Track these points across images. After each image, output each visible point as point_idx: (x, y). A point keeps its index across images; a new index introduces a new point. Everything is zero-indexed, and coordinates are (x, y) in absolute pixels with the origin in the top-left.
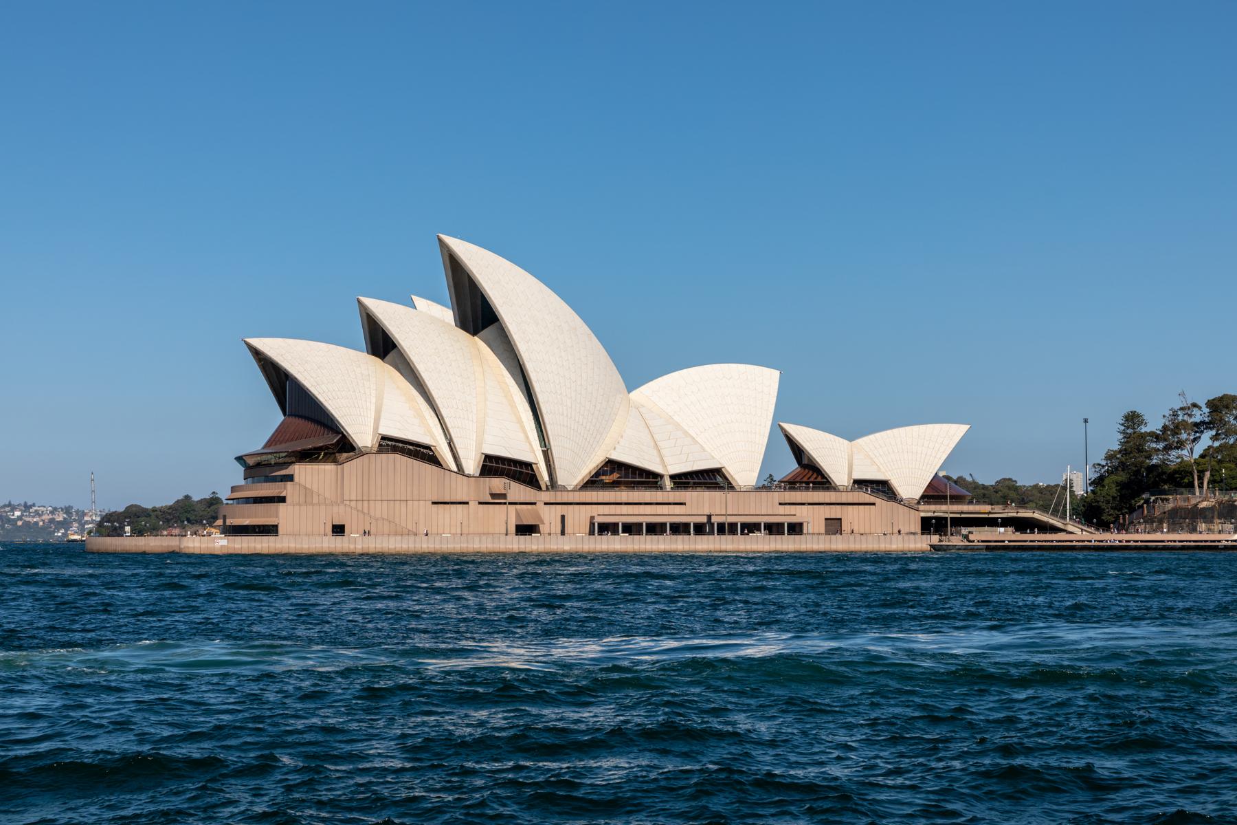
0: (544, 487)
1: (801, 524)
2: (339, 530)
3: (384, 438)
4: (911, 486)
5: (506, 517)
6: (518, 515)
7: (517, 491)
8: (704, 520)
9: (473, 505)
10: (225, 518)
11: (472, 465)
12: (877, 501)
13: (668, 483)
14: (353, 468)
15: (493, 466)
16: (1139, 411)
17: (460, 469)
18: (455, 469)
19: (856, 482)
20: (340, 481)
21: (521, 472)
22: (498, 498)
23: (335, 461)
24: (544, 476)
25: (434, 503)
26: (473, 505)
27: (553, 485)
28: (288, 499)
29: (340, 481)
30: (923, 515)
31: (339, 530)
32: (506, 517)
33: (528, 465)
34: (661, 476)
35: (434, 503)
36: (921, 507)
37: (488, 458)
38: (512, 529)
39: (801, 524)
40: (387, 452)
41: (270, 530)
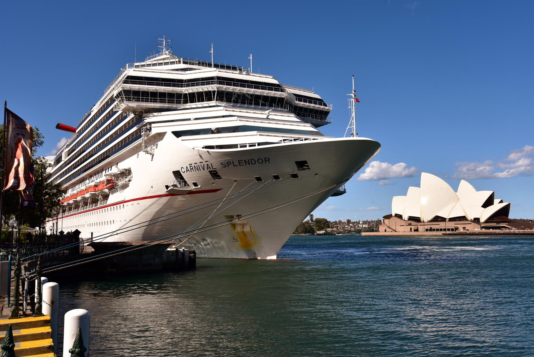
4: (482, 220)
7: (413, 223)
11: (406, 219)
13: (447, 220)
21: (417, 220)
22: (410, 224)
27: (423, 222)
34: (446, 219)
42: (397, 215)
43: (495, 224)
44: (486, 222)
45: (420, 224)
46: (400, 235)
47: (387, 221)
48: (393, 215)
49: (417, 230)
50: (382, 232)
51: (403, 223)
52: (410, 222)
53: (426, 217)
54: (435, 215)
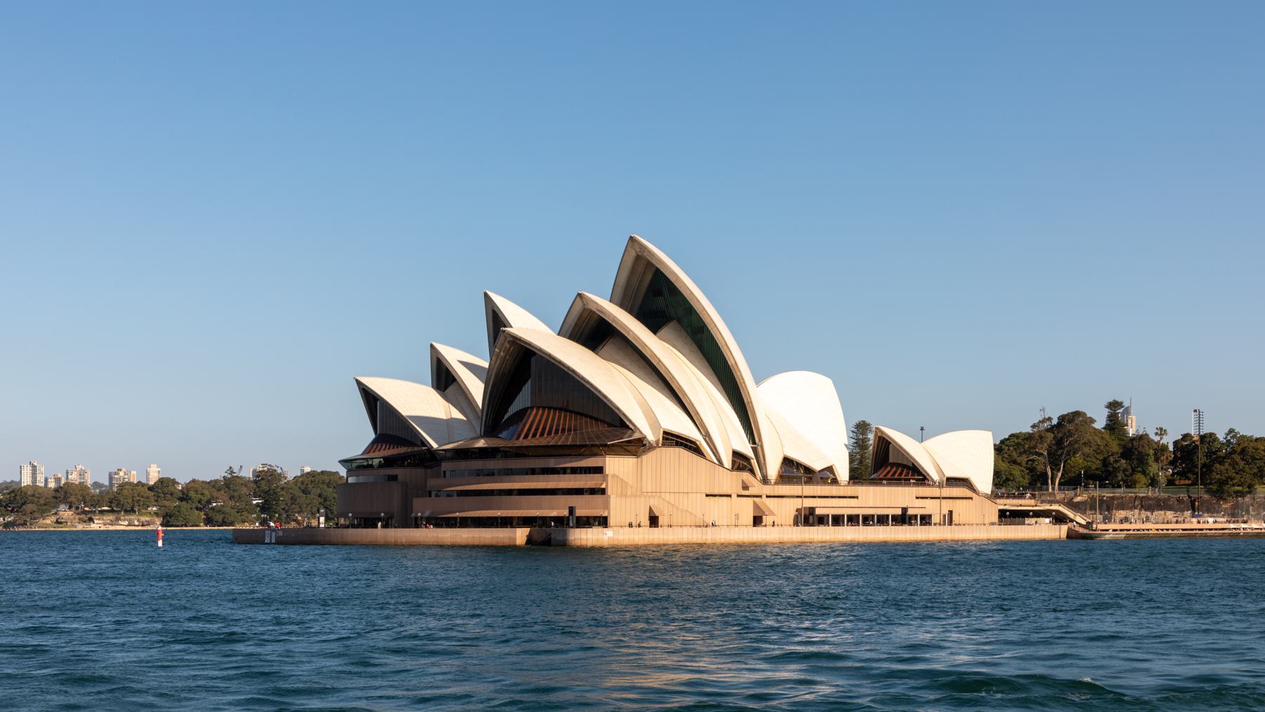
1: (930, 516)
3: (665, 433)
6: (756, 506)
8: (899, 512)
9: (734, 496)
10: (571, 510)
14: (648, 458)
15: (740, 462)
16: (868, 421)
17: (721, 464)
20: (639, 470)
23: (636, 454)
26: (734, 496)
27: (765, 480)
29: (639, 470)
39: (930, 516)
41: (603, 522)
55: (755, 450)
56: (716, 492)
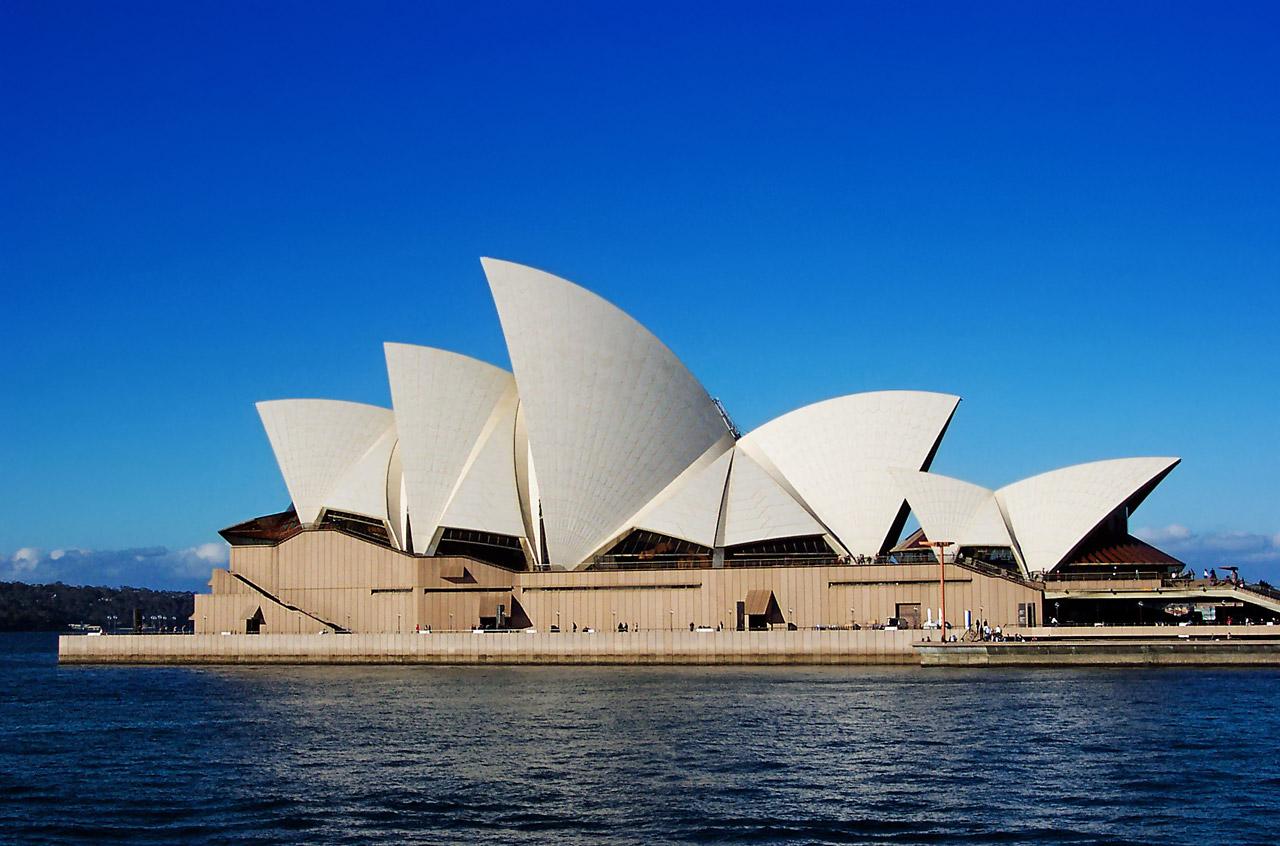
0: (531, 567)
2: (254, 625)
4: (1043, 552)
5: (472, 605)
6: (483, 600)
11: (423, 543)
12: (975, 576)
15: (453, 542)
17: (410, 551)
18: (405, 549)
19: (966, 551)
21: (504, 552)
24: (534, 555)
25: (373, 591)
28: (214, 590)
30: (1048, 596)
31: (254, 625)
32: (472, 605)
33: (514, 540)
35: (373, 591)
36: (1049, 585)
37: (448, 531)
38: (478, 624)
40: (329, 529)
42: (333, 521)
43: (1157, 583)
44: (1067, 568)
45: (524, 579)
46: (646, 661)
47: (253, 558)
48: (308, 515)
49: (516, 619)
50: (216, 633)
51: (405, 571)
52: (456, 564)
53: (575, 535)
54: (621, 530)
55: (541, 521)
56: (388, 586)
